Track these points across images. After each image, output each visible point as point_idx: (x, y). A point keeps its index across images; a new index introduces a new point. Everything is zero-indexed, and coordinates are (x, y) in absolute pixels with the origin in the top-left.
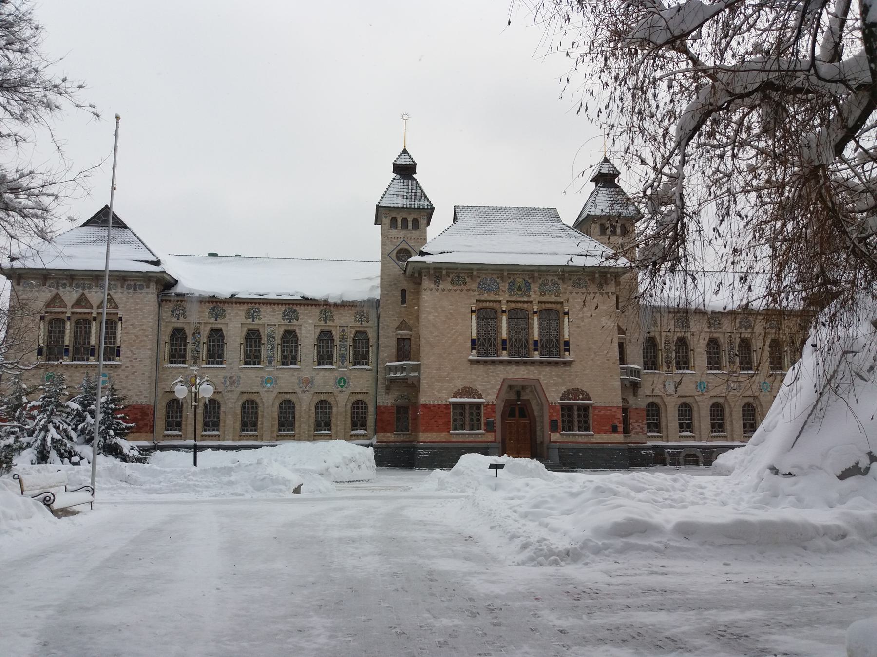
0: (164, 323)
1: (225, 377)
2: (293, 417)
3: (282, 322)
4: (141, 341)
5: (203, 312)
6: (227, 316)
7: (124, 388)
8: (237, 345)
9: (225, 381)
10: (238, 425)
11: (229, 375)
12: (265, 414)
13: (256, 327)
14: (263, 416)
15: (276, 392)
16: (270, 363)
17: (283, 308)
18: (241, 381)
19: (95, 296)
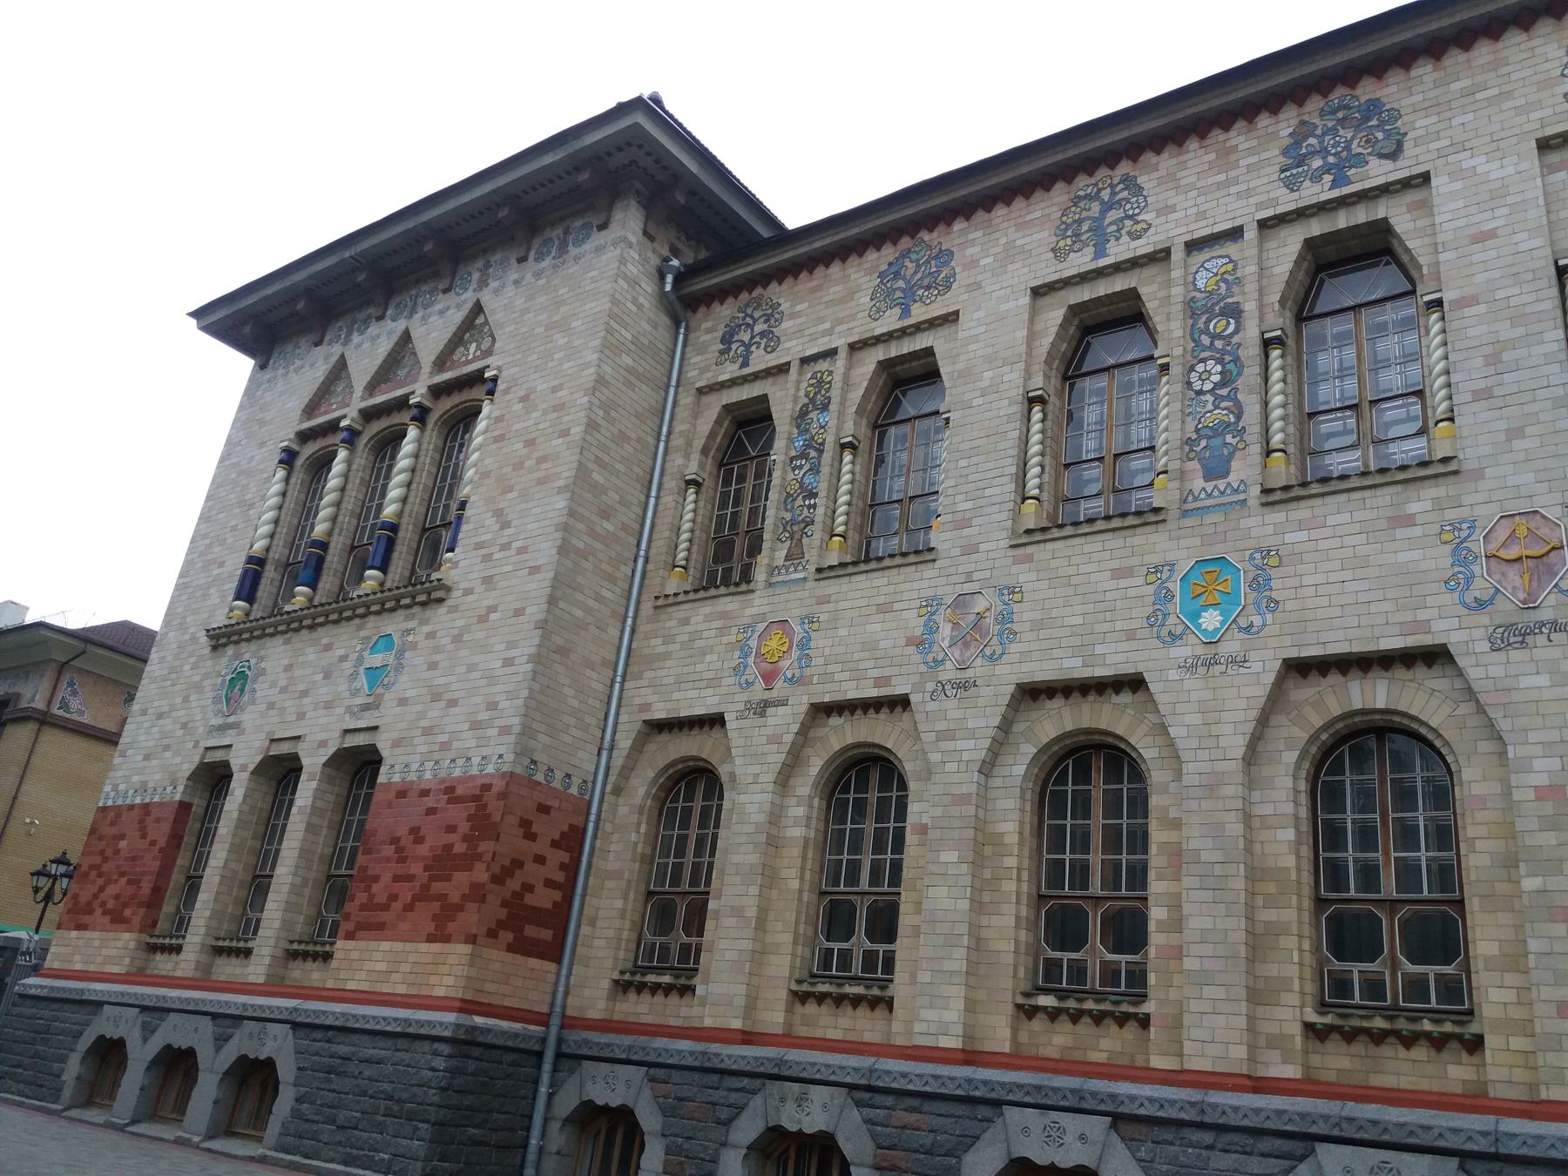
0: (687, 399)
1: (930, 605)
2: (1448, 875)
3: (1288, 202)
4: (540, 460)
5: (850, 296)
6: (962, 278)
7: (436, 697)
8: (1007, 406)
9: (931, 629)
10: (1009, 927)
11: (949, 594)
12: (1195, 839)
13: (1118, 284)
14: (1177, 855)
15: (1264, 668)
16: (1216, 470)
17: (1284, 124)
18: (1025, 615)
19: (432, 324)
